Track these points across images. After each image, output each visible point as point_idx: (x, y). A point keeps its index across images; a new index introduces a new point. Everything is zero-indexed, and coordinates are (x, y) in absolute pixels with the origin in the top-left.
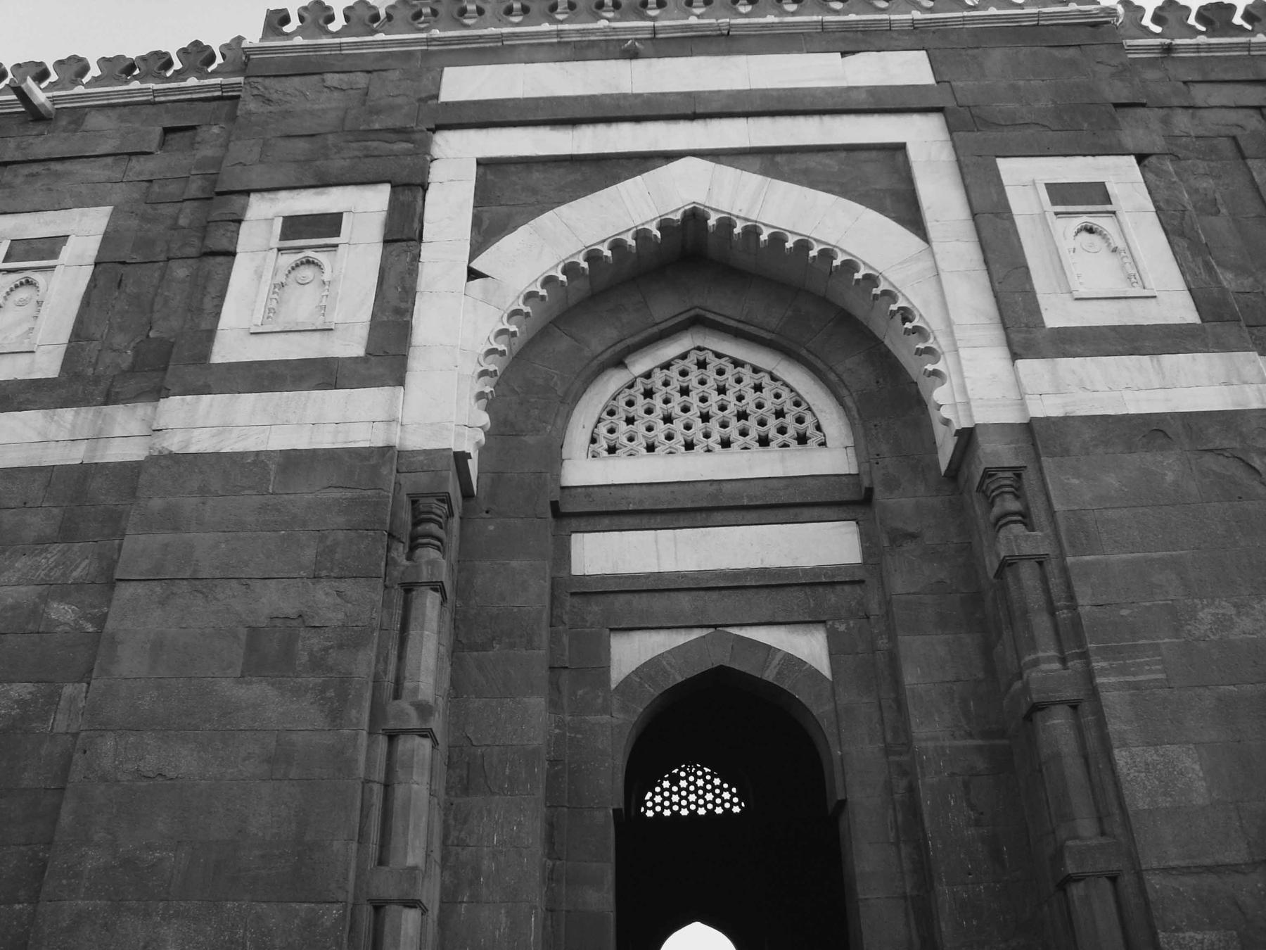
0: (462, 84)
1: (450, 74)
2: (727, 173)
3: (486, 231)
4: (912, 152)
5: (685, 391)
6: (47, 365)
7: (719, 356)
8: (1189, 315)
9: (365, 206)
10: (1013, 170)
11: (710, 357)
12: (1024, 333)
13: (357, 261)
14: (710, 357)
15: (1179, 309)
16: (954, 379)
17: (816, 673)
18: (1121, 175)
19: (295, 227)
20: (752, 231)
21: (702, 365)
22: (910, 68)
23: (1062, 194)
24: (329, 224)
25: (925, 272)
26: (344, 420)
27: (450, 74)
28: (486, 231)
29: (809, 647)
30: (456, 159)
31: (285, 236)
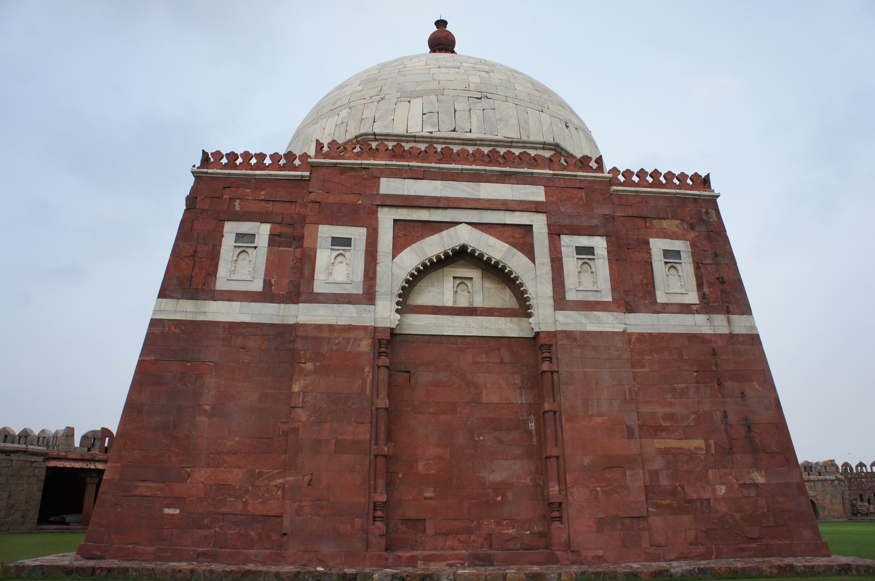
0: (389, 186)
1: (383, 181)
2: (476, 232)
3: (397, 249)
4: (534, 227)
6: (257, 286)
8: (609, 298)
9: (358, 234)
12: (560, 302)
13: (357, 255)
18: (599, 244)
20: (481, 255)
22: (537, 194)
23: (580, 250)
27: (383, 181)
28: (397, 249)
30: (386, 219)
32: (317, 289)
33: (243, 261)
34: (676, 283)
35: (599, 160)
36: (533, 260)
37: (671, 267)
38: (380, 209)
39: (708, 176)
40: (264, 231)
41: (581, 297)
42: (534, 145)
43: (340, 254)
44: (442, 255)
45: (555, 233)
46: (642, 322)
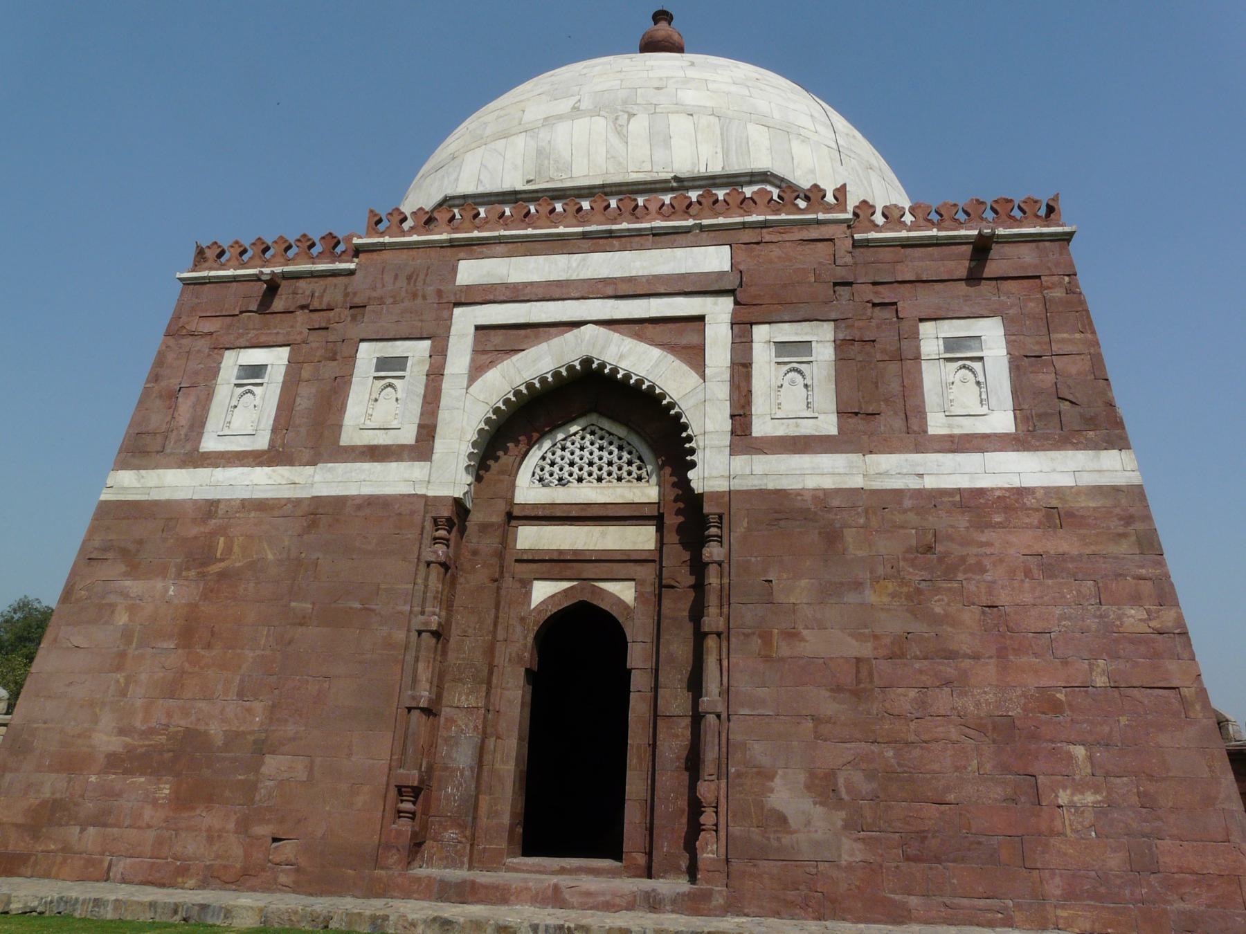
5: (582, 449)
7: (602, 429)
9: (418, 350)
10: (761, 333)
11: (597, 430)
13: (413, 382)
14: (597, 430)
15: (828, 425)
16: (699, 465)
17: (626, 606)
19: (384, 364)
21: (593, 433)
24: (398, 363)
25: (700, 400)
29: (624, 592)
31: (377, 370)
32: (345, 440)
33: (244, 401)
35: (841, 192)
37: (964, 367)
38: (458, 311)
39: (1056, 198)
40: (276, 359)
41: (780, 430)
43: (390, 385)
44: (549, 376)
45: (742, 327)
46: (893, 470)
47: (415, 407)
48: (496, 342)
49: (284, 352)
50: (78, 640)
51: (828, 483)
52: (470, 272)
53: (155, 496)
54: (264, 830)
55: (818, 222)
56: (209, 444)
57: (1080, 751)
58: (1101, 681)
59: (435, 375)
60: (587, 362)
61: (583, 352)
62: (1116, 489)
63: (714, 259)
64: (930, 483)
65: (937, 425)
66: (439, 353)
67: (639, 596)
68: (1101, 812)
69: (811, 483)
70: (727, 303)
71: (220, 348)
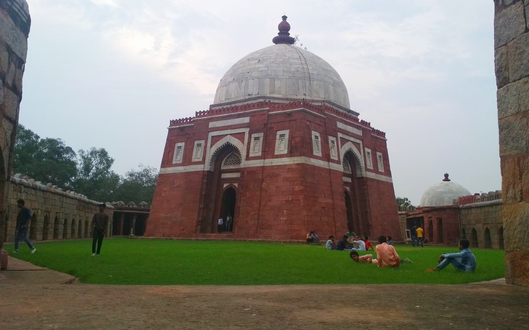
6: (181, 162)
9: (203, 142)
18: (261, 135)
26: (199, 168)
29: (236, 185)
34: (282, 146)
36: (243, 143)
42: (255, 99)
47: (202, 154)
48: (215, 139)
49: (184, 143)
50: (158, 199)
51: (258, 165)
52: (211, 125)
53: (167, 173)
54: (181, 228)
55: (264, 111)
56: (174, 162)
57: (285, 211)
58: (290, 199)
59: (206, 147)
60: (228, 142)
61: (228, 140)
62: (298, 164)
63: (247, 120)
64: (273, 164)
65: (276, 153)
66: (206, 143)
67: (239, 185)
68: (286, 221)
69: (256, 165)
70: (248, 129)
71: (175, 143)
